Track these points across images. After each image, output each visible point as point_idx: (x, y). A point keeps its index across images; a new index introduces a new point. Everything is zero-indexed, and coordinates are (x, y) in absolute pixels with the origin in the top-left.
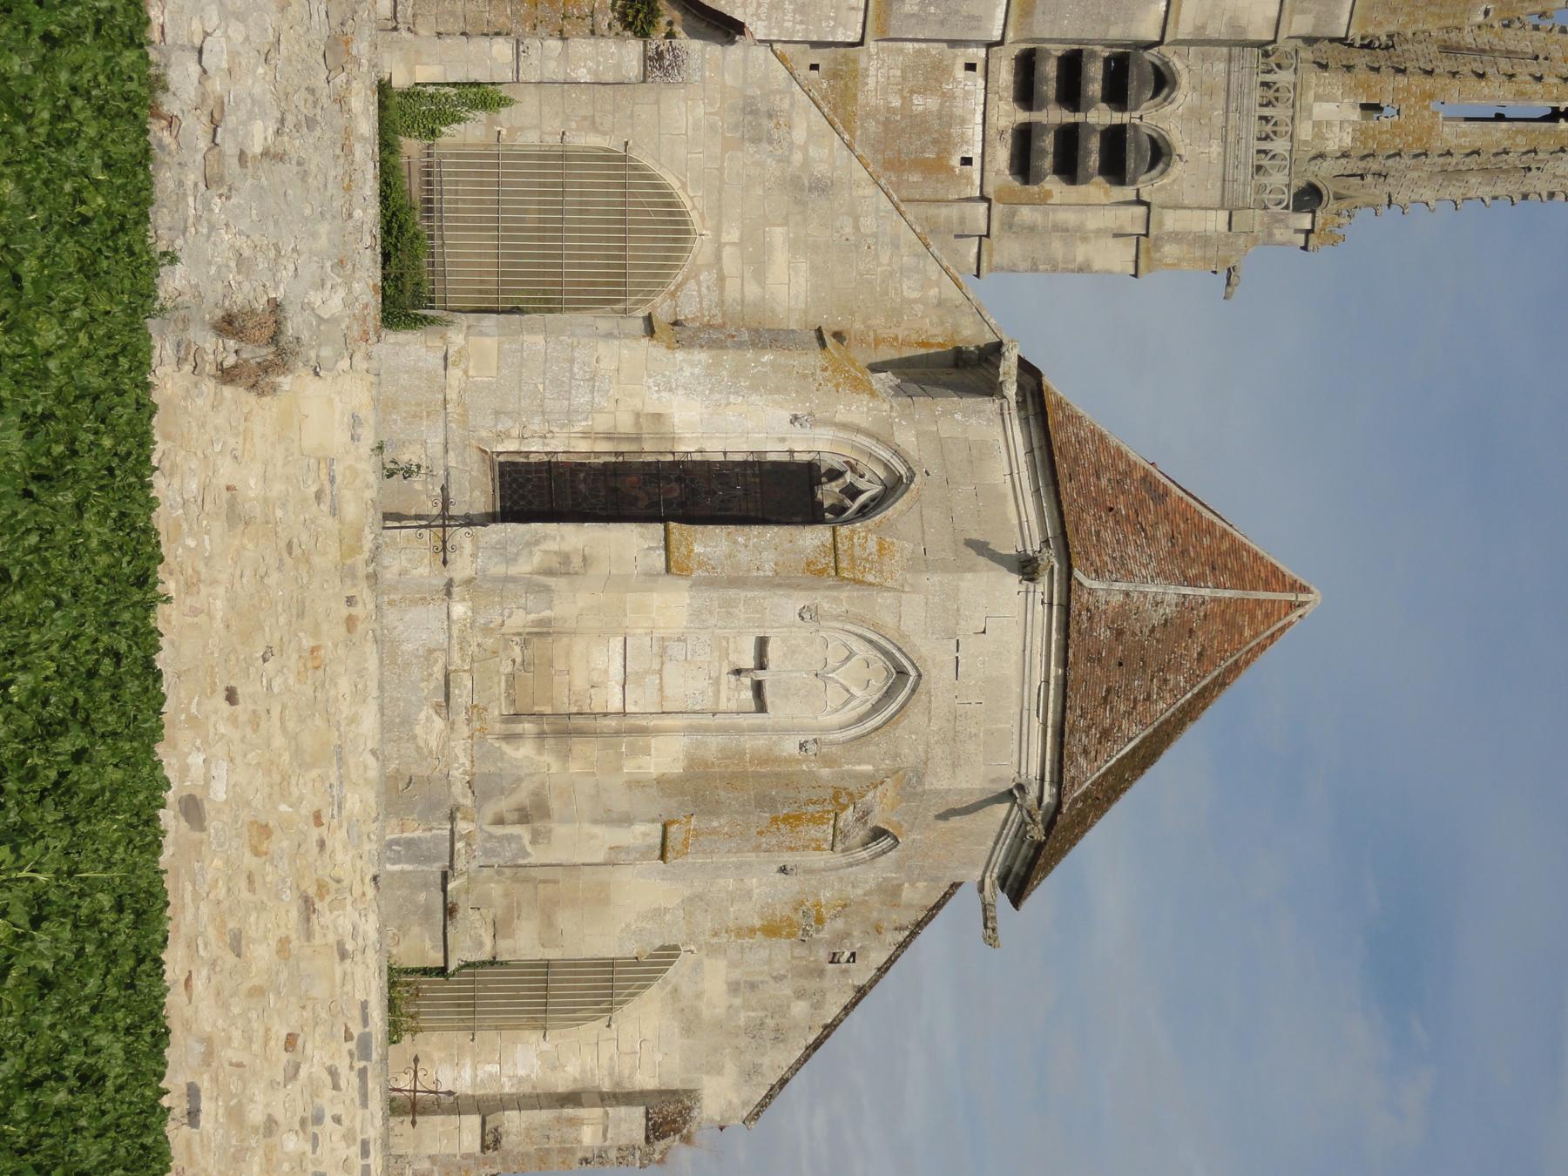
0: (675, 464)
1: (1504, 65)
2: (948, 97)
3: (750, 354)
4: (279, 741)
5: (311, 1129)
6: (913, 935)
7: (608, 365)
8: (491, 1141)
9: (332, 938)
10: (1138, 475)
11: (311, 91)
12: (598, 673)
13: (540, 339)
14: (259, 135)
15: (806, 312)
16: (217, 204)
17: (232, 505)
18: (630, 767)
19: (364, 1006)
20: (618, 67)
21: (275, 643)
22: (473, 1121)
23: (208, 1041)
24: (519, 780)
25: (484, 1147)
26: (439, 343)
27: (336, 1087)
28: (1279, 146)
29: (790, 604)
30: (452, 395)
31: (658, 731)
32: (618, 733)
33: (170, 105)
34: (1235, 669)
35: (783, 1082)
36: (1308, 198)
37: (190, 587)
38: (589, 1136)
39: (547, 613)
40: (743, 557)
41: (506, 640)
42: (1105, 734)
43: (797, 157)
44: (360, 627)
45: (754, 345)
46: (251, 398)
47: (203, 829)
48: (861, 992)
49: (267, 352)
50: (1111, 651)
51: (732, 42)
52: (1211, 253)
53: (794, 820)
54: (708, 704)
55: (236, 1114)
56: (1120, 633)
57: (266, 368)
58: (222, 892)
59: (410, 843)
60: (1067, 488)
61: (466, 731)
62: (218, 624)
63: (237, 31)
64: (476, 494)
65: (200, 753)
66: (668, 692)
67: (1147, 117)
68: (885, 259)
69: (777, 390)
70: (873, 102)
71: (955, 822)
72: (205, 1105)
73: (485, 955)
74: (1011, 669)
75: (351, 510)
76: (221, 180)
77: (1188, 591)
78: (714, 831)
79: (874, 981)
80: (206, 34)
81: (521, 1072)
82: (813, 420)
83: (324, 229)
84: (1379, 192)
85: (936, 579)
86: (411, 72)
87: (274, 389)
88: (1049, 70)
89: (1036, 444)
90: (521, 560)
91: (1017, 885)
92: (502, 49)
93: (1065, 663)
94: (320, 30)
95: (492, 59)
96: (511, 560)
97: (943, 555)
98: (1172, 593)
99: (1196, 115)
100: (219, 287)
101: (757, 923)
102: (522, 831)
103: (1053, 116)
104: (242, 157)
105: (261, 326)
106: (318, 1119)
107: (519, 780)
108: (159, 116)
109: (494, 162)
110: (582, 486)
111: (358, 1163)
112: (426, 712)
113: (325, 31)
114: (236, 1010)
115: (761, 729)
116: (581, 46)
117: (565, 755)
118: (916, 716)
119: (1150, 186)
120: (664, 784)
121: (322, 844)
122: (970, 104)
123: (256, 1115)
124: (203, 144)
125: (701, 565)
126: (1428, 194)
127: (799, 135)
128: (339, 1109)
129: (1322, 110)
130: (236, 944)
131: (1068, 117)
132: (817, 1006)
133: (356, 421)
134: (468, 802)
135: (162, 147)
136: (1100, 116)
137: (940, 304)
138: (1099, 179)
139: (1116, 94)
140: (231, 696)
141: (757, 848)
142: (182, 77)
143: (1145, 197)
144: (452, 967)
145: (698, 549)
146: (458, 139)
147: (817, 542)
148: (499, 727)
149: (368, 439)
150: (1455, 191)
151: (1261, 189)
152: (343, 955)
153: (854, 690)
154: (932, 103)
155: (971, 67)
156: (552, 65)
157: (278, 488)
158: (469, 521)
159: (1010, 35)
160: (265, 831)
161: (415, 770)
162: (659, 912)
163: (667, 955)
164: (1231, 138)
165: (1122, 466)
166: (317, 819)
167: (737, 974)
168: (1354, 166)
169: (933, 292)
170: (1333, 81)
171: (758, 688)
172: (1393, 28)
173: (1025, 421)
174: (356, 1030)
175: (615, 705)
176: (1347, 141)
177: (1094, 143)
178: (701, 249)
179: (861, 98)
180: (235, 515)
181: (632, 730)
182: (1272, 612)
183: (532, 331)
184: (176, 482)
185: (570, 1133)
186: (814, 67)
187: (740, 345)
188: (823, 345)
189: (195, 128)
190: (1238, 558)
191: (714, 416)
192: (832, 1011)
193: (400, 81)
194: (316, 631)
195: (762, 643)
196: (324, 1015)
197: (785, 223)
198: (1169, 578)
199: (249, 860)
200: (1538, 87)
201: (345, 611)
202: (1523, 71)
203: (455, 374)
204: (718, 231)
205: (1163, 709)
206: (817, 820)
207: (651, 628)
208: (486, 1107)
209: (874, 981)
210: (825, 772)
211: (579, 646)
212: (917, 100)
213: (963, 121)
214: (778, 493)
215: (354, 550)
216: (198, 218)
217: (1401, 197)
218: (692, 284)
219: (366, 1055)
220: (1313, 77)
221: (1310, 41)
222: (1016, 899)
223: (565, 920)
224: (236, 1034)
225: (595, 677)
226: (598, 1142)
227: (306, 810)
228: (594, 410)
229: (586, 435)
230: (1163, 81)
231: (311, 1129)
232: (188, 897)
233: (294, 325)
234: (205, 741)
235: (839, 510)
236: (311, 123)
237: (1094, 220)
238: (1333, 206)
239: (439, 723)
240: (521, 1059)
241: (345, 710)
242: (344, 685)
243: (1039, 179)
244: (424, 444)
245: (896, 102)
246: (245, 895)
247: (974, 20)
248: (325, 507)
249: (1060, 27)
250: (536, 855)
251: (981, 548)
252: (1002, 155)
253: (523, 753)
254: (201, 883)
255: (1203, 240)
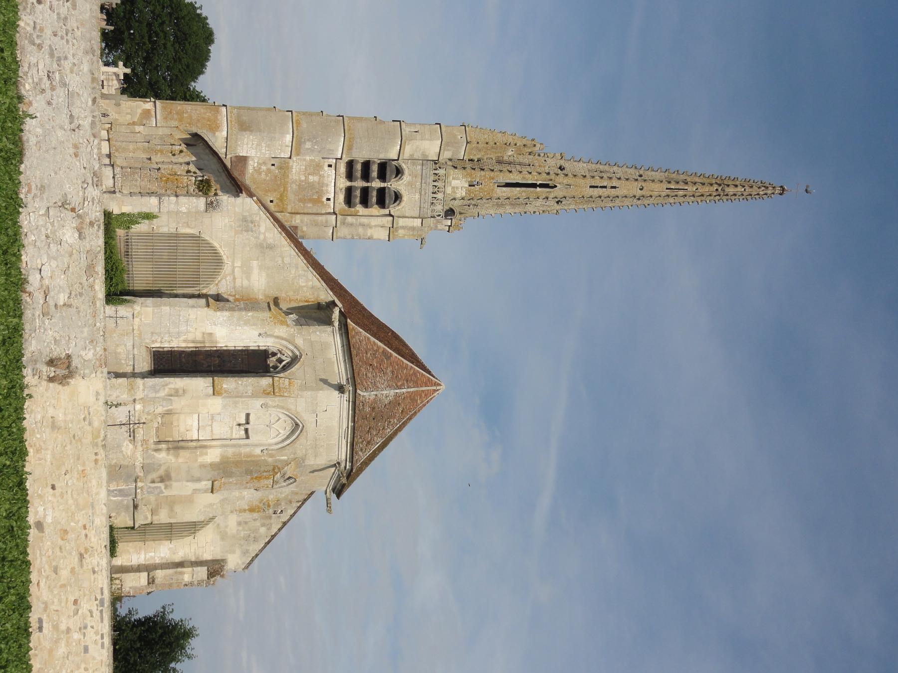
0: (217, 351)
1: (518, 167)
2: (322, 176)
3: (244, 313)
4: (71, 501)
5: (83, 631)
6: (303, 504)
7: (193, 316)
8: (151, 581)
9: (90, 567)
10: (381, 351)
11: (81, 284)
12: (189, 426)
13: (168, 308)
14: (62, 299)
16: (47, 322)
17: (53, 423)
18: (200, 460)
19: (102, 589)
20: (197, 207)
21: (69, 469)
22: (145, 574)
23: (46, 603)
24: (160, 465)
25: (149, 583)
26: (131, 310)
27: (92, 616)
28: (440, 196)
29: (258, 402)
30: (136, 327)
31: (211, 447)
32: (196, 448)
33: (29, 288)
34: (415, 413)
35: (257, 555)
36: (450, 213)
37: (38, 451)
38: (187, 578)
39: (170, 407)
40: (241, 388)
41: (156, 416)
42: (368, 443)
43: (262, 237)
44: (100, 463)
45: (245, 309)
46: (60, 387)
47: (43, 532)
48: (285, 524)
49: (66, 372)
50: (370, 415)
51: (238, 196)
52: (415, 233)
53: (259, 478)
54: (229, 436)
55: (56, 627)
56: (374, 408)
57: (65, 377)
58: (50, 553)
59: (120, 490)
60: (356, 359)
61: (141, 449)
62: (48, 463)
63: (54, 264)
64: (145, 365)
65: (42, 508)
66: (214, 432)
67: (393, 185)
68: (293, 272)
69: (254, 325)
70: (295, 178)
71: (316, 473)
72: (45, 625)
73: (149, 521)
74: (335, 423)
75: (96, 424)
76: (48, 314)
77: (398, 391)
78: (231, 483)
79: (289, 520)
80: (43, 265)
81: (162, 555)
82: (266, 335)
83: (86, 330)
84: (475, 211)
85: (309, 393)
86: (120, 209)
87: (68, 384)
88: (359, 167)
91: (339, 491)
92: (154, 200)
93: (354, 421)
94: (84, 263)
95: (151, 204)
96: (157, 392)
98: (392, 392)
99: (410, 184)
100: (48, 349)
101: (247, 507)
102: (162, 485)
103: (360, 184)
104: (56, 305)
105: (63, 363)
106: (85, 627)
107: (160, 465)
108: (26, 292)
109: (151, 236)
110: (184, 360)
111: (101, 641)
112: (126, 442)
113: (86, 263)
114: (56, 592)
115: (247, 445)
116: (183, 199)
117: (177, 456)
118: (302, 440)
119: (394, 209)
120: (213, 466)
121: (86, 536)
122: (330, 179)
123: (63, 627)
124: (42, 302)
125: (226, 392)
126: (492, 212)
127: (262, 229)
128: (93, 624)
129: (455, 183)
130: (56, 570)
131: (365, 184)
132: (269, 529)
133: (98, 393)
134: (142, 474)
135: (26, 302)
136: (377, 184)
137: (313, 287)
138: (376, 206)
139: (382, 176)
140: (53, 487)
141: (246, 488)
142: (34, 280)
143: (392, 213)
144: (136, 526)
145: (225, 386)
146: (138, 230)
148: (153, 446)
149: (102, 400)
150: (501, 211)
151: (433, 211)
152: (94, 572)
153: (281, 431)
154: (316, 178)
155: (330, 166)
156: (172, 206)
157: (70, 417)
158: (143, 376)
159: (344, 156)
160: (66, 532)
161: (122, 463)
162: (211, 505)
163: (213, 518)
164: (423, 193)
165: (375, 348)
166: (85, 527)
167: (240, 519)
168: (466, 202)
169: (310, 283)
170: (458, 173)
171: (246, 430)
172: (479, 156)
173: (341, 335)
174: (99, 597)
175: (195, 437)
176: (464, 194)
177: (374, 193)
178: (227, 269)
179: (290, 177)
180: (54, 426)
181: (200, 446)
182: (427, 394)
183: (165, 305)
184: (33, 416)
185: (180, 577)
186: (273, 165)
187: (240, 310)
188: (270, 309)
189: (39, 297)
190: (416, 376)
191: (230, 333)
192: (274, 530)
193: (116, 211)
194: (84, 464)
195: (248, 415)
196: (87, 592)
197: (258, 260)
198: (389, 386)
199: (60, 542)
200: (530, 176)
201: (94, 457)
202: (525, 170)
203: (137, 320)
204: (233, 262)
205: (389, 431)
206: (267, 478)
207: (206, 410)
208: (149, 568)
209: (289, 520)
210: (270, 460)
211: (182, 417)
212: (311, 177)
213: (327, 185)
214: (252, 363)
215: (98, 437)
216: (40, 327)
217: (483, 212)
219: (102, 605)
220: (452, 172)
221: (450, 160)
222: (338, 496)
223: (178, 509)
224: (56, 601)
225: (188, 428)
226: (190, 580)
227: (81, 524)
228: (188, 332)
229: (185, 341)
230: (399, 172)
231: (83, 631)
232: (38, 555)
233: (75, 362)
234: (44, 503)
235: (275, 367)
236: (81, 294)
237: (374, 221)
238: (458, 216)
239: (131, 446)
240: (162, 551)
241: (94, 490)
242: (94, 482)
243: (355, 206)
244: (126, 345)
245: (303, 178)
246: (59, 553)
247: (331, 151)
248: (87, 423)
249: (360, 156)
250: (167, 493)
251: (325, 381)
252: (341, 197)
253: (162, 456)
254: (41, 551)
255: (413, 228)
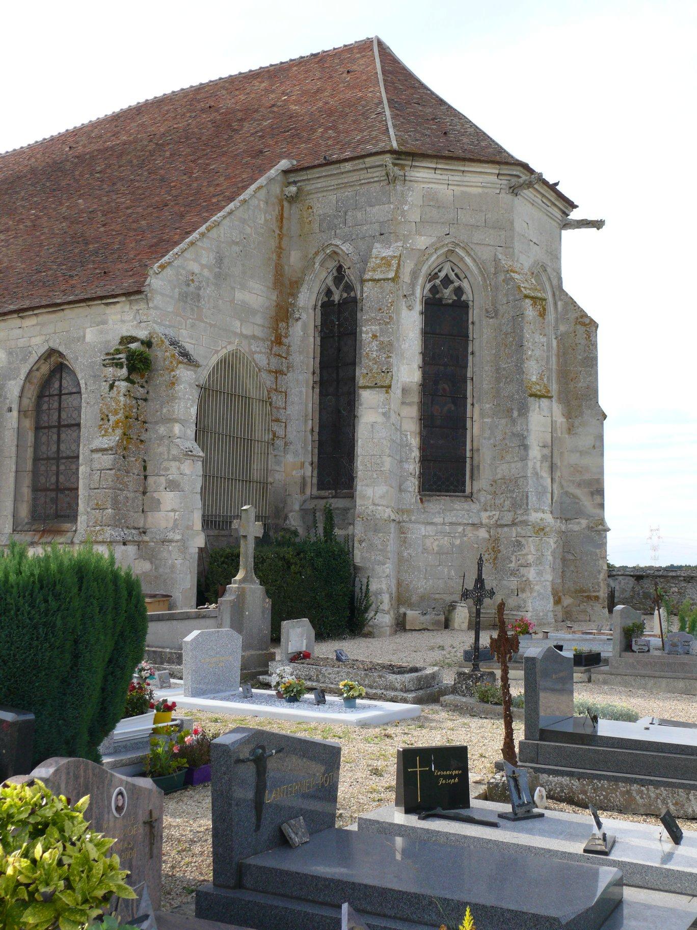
15: (268, 287)
89: (434, 166)
90: (545, 484)
97: (503, 237)
110: (440, 442)
145: (534, 379)
147: (531, 308)
218: (256, 356)
